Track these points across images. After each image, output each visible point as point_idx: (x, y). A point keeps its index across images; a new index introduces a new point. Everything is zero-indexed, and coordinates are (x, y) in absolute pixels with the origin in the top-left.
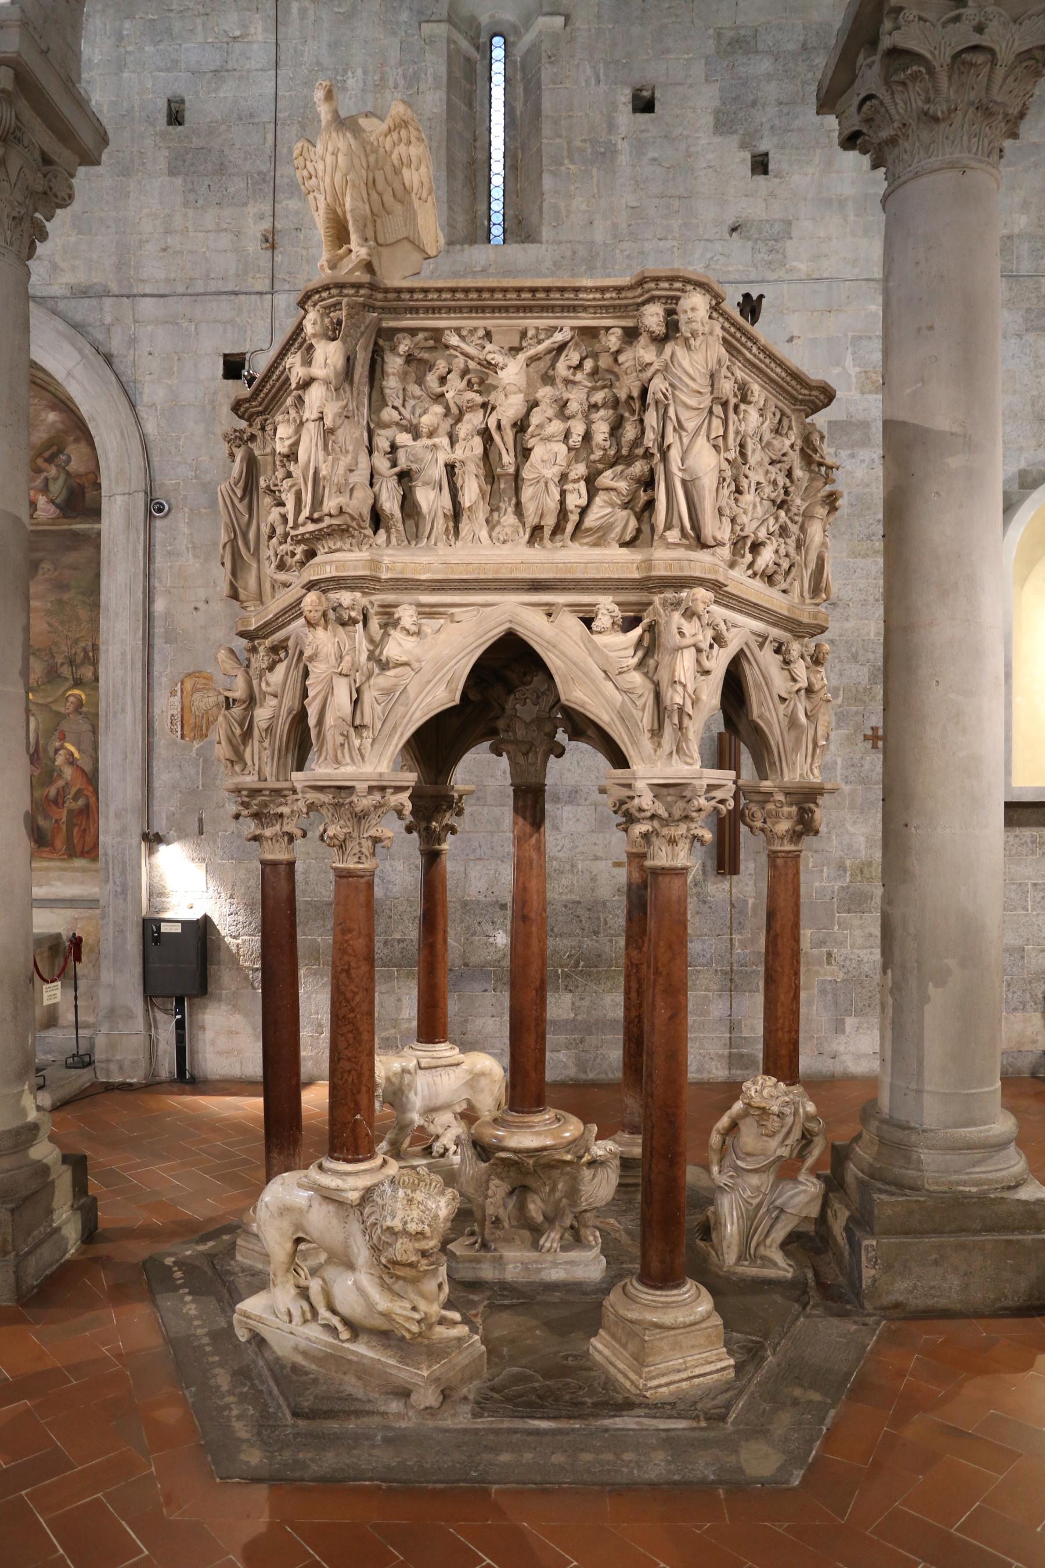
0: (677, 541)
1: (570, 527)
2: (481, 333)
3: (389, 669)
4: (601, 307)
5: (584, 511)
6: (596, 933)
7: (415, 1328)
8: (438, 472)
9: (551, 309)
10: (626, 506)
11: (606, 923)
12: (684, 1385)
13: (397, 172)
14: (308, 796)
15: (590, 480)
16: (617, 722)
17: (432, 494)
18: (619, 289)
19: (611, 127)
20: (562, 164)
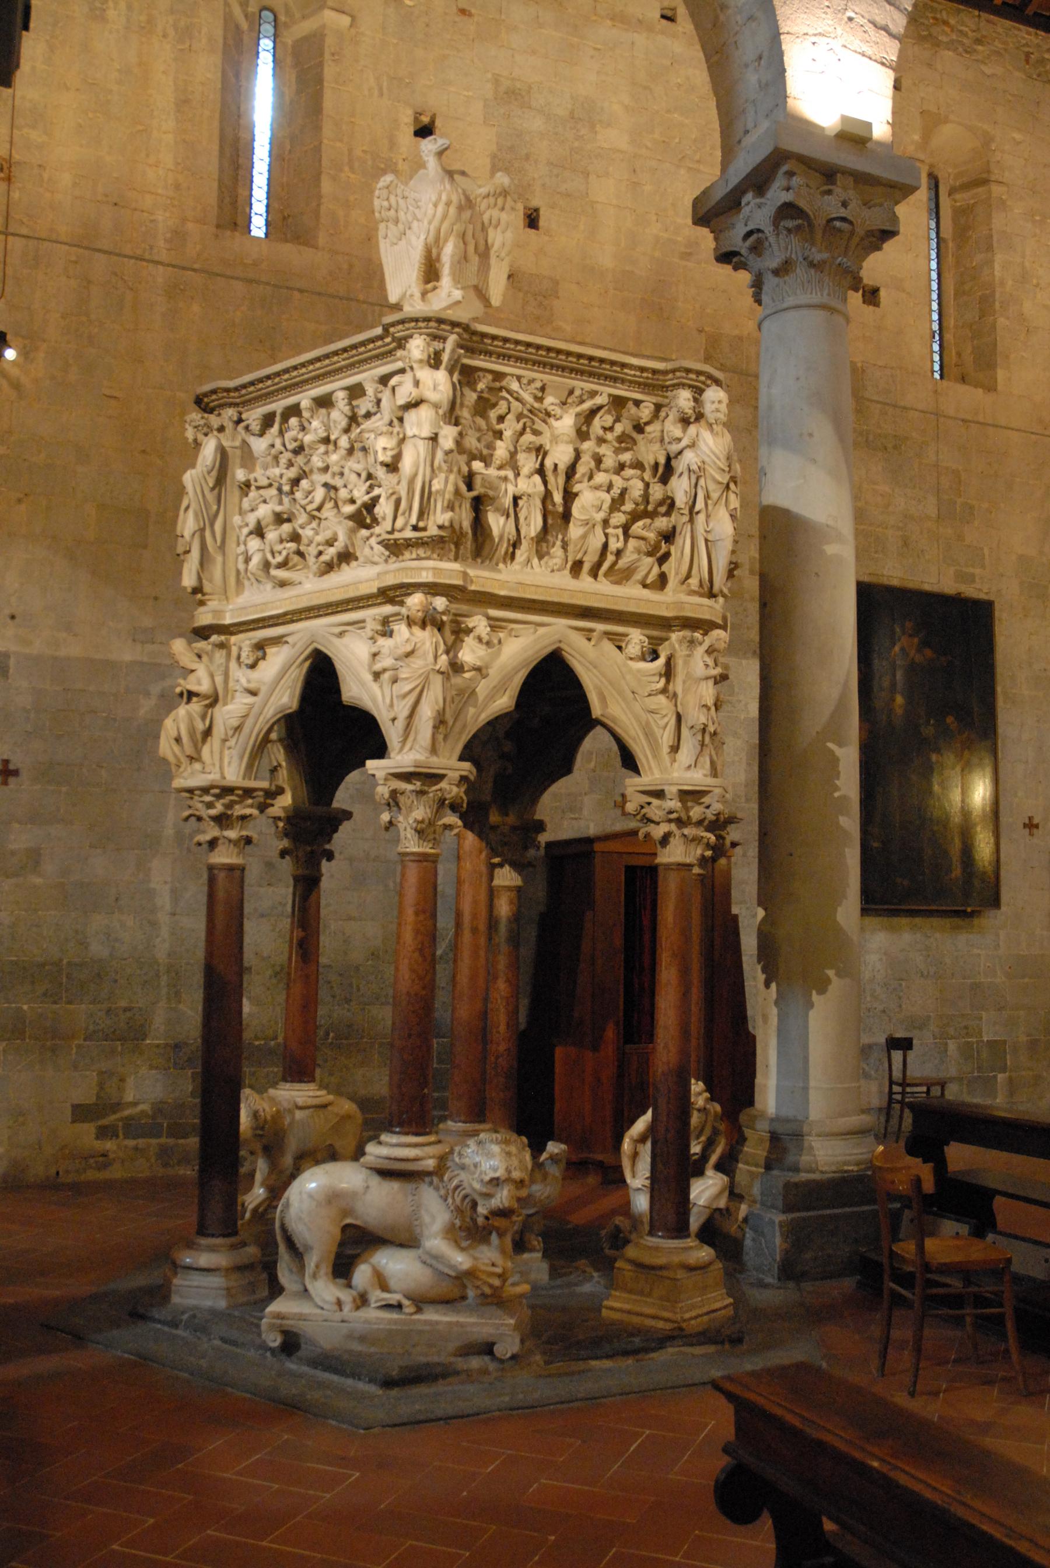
0: (696, 589)
1: (606, 566)
2: (539, 385)
3: (464, 672)
4: (636, 382)
5: (619, 553)
6: (348, 1001)
7: (497, 1282)
8: (508, 501)
9: (599, 376)
10: (649, 554)
11: (359, 990)
12: (706, 1318)
13: (484, 229)
14: (389, 783)
15: (626, 528)
16: (642, 737)
17: (502, 520)
18: (654, 372)
19: (392, 144)
20: (341, 170)
